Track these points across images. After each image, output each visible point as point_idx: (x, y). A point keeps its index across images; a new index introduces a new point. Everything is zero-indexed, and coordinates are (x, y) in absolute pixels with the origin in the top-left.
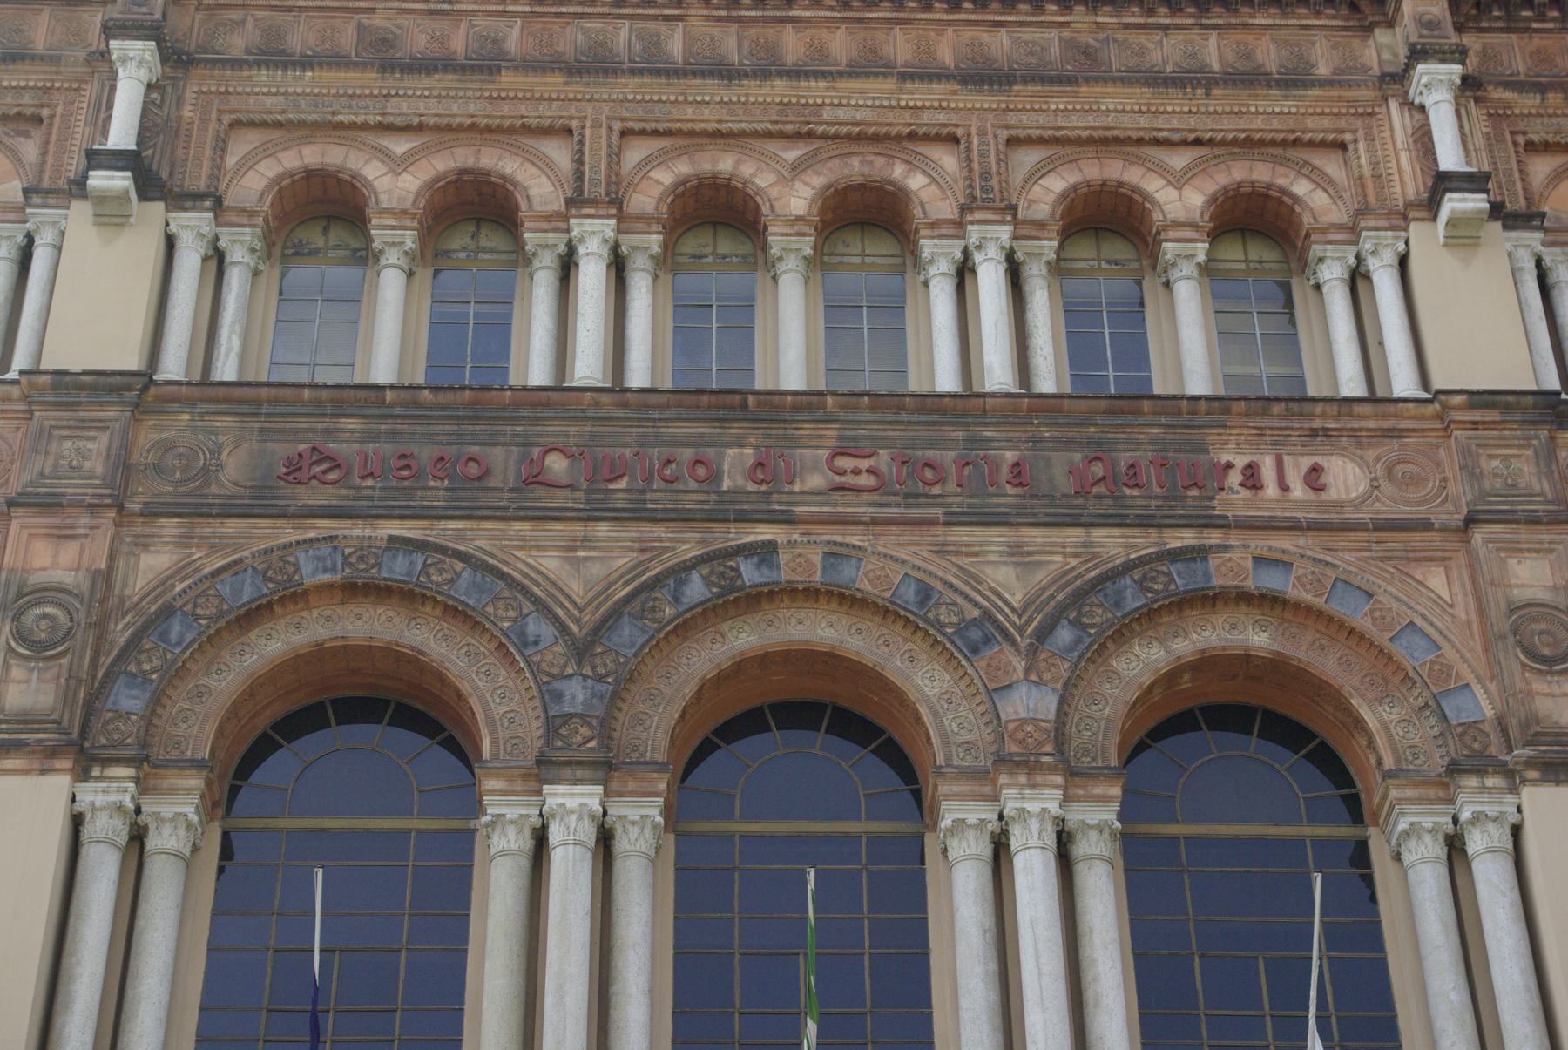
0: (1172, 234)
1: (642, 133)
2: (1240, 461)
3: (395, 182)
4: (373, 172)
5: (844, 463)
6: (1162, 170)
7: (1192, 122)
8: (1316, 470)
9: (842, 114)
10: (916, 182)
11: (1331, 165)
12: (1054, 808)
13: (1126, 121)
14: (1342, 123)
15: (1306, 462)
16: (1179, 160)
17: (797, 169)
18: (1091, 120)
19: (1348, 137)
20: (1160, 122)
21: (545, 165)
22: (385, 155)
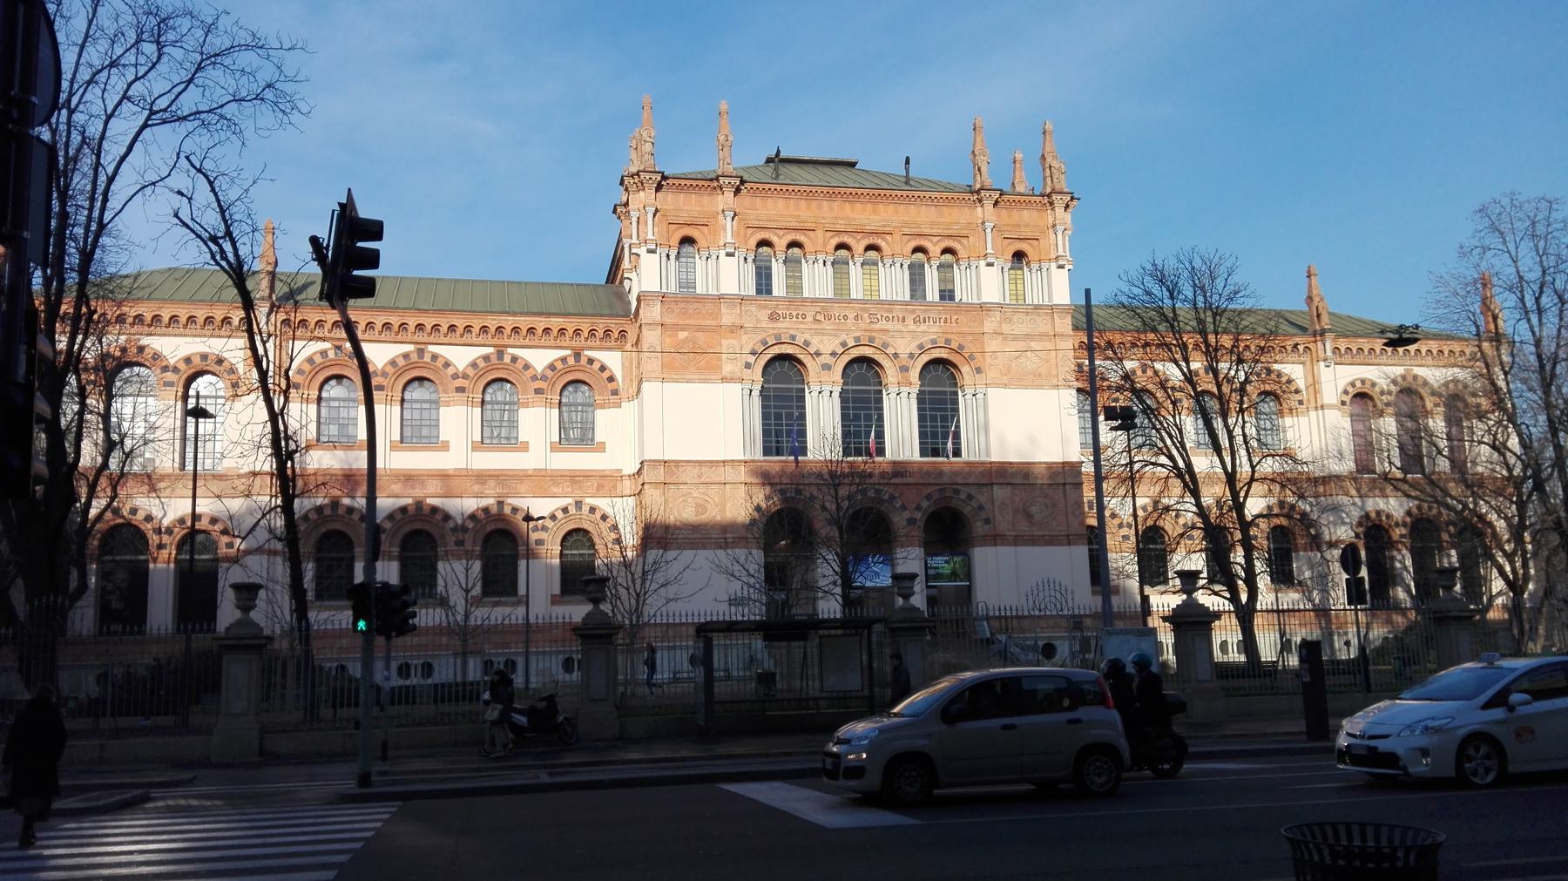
3: (780, 242)
4: (775, 239)
10: (883, 244)
11: (964, 241)
16: (935, 239)
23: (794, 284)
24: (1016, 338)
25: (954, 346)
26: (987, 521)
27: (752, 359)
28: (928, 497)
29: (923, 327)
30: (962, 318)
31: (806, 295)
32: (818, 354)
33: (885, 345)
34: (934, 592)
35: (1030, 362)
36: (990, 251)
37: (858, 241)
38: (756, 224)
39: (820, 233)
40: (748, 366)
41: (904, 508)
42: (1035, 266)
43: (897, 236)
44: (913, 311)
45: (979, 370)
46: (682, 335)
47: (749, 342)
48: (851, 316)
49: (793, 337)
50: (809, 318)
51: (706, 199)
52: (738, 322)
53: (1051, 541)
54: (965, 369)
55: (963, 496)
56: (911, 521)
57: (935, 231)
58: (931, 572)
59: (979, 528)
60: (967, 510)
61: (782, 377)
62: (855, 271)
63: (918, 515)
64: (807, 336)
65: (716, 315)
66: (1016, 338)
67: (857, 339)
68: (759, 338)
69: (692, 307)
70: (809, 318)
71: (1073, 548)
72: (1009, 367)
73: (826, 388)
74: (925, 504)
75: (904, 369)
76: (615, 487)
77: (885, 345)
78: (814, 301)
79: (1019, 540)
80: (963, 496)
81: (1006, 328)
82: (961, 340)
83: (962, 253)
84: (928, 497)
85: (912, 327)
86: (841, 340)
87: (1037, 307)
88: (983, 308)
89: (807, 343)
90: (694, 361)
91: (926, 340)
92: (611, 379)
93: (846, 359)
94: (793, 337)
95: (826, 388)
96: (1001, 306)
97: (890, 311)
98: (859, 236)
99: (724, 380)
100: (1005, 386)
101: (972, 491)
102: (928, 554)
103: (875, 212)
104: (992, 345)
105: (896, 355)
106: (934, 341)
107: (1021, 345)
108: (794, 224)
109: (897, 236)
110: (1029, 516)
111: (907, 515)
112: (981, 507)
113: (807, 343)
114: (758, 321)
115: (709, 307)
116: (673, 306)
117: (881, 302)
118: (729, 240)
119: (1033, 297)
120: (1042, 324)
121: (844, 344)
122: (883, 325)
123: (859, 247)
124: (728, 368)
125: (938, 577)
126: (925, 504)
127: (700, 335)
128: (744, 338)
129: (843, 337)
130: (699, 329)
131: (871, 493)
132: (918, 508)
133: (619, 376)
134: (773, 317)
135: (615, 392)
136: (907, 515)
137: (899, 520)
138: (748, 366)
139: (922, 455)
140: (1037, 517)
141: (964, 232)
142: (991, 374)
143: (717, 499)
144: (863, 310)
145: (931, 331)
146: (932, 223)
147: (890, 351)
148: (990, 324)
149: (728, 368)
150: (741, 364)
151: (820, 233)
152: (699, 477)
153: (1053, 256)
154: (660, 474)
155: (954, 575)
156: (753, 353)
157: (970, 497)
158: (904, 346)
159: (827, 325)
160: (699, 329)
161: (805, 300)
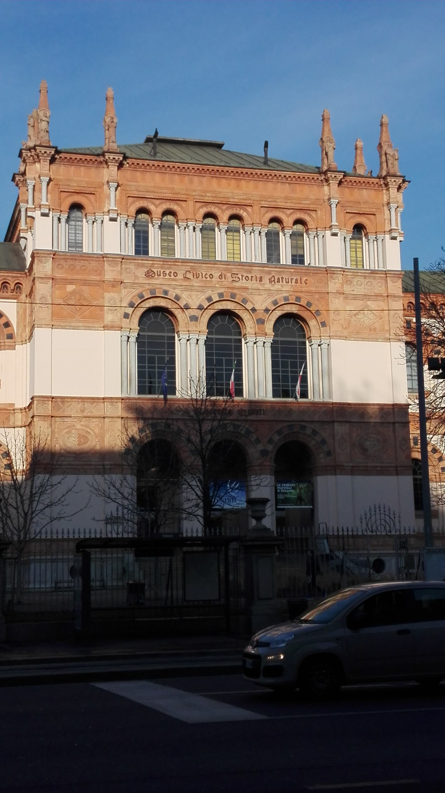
0: (287, 228)
3: (157, 210)
4: (152, 207)
5: (233, 276)
7: (292, 205)
8: (306, 280)
9: (233, 200)
10: (244, 214)
11: (313, 214)
13: (280, 204)
14: (316, 207)
15: (305, 278)
16: (289, 212)
18: (275, 203)
19: (317, 209)
20: (287, 205)
21: (181, 207)
22: (154, 204)
23: (168, 246)
24: (355, 297)
25: (303, 302)
26: (329, 454)
27: (130, 310)
28: (279, 432)
29: (277, 286)
30: (311, 280)
31: (177, 256)
32: (187, 307)
33: (245, 301)
34: (283, 514)
35: (367, 318)
36: (334, 223)
37: (223, 211)
38: (136, 194)
39: (191, 203)
40: (126, 316)
41: (258, 441)
42: (372, 237)
43: (256, 208)
44: (269, 272)
45: (324, 324)
46: (70, 288)
47: (127, 295)
48: (216, 275)
49: (166, 292)
50: (180, 276)
51: (93, 172)
52: (119, 278)
53: (382, 471)
54: (312, 323)
55: (309, 431)
56: (264, 453)
57: (289, 205)
58: (280, 497)
59: (322, 459)
60: (312, 444)
61: (155, 329)
62: (220, 237)
63: (270, 448)
64: (178, 292)
65: (101, 272)
66: (355, 297)
67: (221, 295)
68: (136, 292)
69: (78, 264)
70: (180, 276)
71: (400, 477)
72: (349, 322)
73: (193, 337)
74: (276, 438)
75: (261, 322)
76: (8, 419)
77: (245, 301)
78: (185, 261)
79: (354, 471)
80: (309, 431)
81: (347, 289)
82: (309, 298)
83: (311, 224)
84: (279, 432)
85: (268, 286)
86: (207, 295)
87: (373, 272)
88: (329, 271)
89: (178, 298)
90: (78, 310)
91: (279, 297)
92: (7, 325)
93: (211, 312)
94: (166, 292)
95: (193, 337)
96: (343, 270)
97: (250, 272)
98: (224, 207)
99: (106, 328)
100: (346, 338)
102: (278, 481)
103: (238, 187)
104: (336, 303)
105: (254, 310)
106: (286, 298)
107: (359, 304)
108: (169, 195)
109: (256, 208)
110: (364, 450)
111: (260, 447)
112: (323, 442)
113: (178, 298)
114: (136, 277)
115: (94, 264)
116: (62, 262)
117: (241, 264)
118: (113, 207)
119: (370, 263)
120: (377, 287)
121: (209, 299)
122: (243, 283)
123: (224, 216)
124: (109, 317)
125: (286, 501)
126: (276, 438)
127: (85, 289)
128: (124, 292)
129: (209, 293)
130: (85, 283)
131: (230, 428)
132: (270, 441)
133: (14, 322)
135: (10, 336)
136: (260, 447)
137: (253, 452)
138: (126, 316)
139: (274, 396)
141: (312, 207)
142: (334, 327)
143: (97, 431)
144: (228, 270)
145: (284, 290)
147: (249, 306)
149: (109, 317)
150: (120, 313)
151: (191, 203)
152: (83, 411)
153: (387, 229)
154: (48, 408)
155: (300, 500)
156: (131, 305)
157: (315, 433)
159: (196, 283)
160: (85, 283)
161: (177, 260)
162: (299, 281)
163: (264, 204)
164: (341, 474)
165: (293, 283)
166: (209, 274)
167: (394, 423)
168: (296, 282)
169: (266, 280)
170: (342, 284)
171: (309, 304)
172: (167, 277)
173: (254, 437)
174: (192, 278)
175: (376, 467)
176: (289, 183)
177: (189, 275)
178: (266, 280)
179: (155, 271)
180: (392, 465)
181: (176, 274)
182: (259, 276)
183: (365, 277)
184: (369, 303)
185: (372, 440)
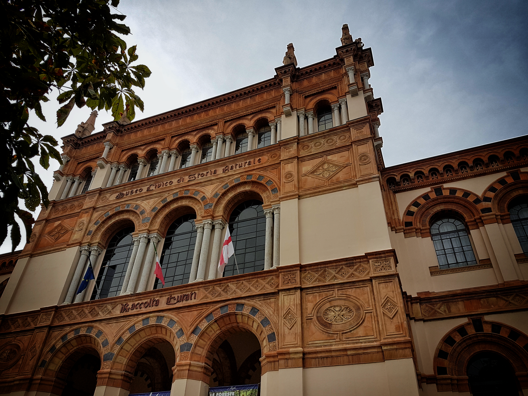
1: (175, 136)
2: (248, 161)
6: (248, 119)
8: (260, 159)
12: (210, 222)
16: (250, 117)
17: (196, 135)
43: (221, 124)
70: (145, 189)
94: (128, 205)
97: (206, 169)
101: (257, 303)
105: (204, 198)
110: (326, 325)
112: (265, 322)
113: (137, 207)
131: (152, 321)
134: (118, 198)
140: (338, 326)
144: (185, 175)
146: (247, 108)
148: (284, 155)
158: (209, 191)
162: (252, 163)
163: (228, 118)
164: (287, 367)
165: (247, 166)
166: (169, 182)
167: (371, 280)
168: (249, 163)
169: (220, 171)
170: (298, 150)
171: (261, 177)
172: (134, 194)
173: (175, 329)
174: (154, 189)
175: (346, 350)
176: (251, 97)
177: (152, 188)
178: (220, 171)
179: (125, 192)
180: (375, 344)
181: (141, 190)
182: (213, 170)
183: (325, 137)
184: (329, 157)
185: (337, 309)
